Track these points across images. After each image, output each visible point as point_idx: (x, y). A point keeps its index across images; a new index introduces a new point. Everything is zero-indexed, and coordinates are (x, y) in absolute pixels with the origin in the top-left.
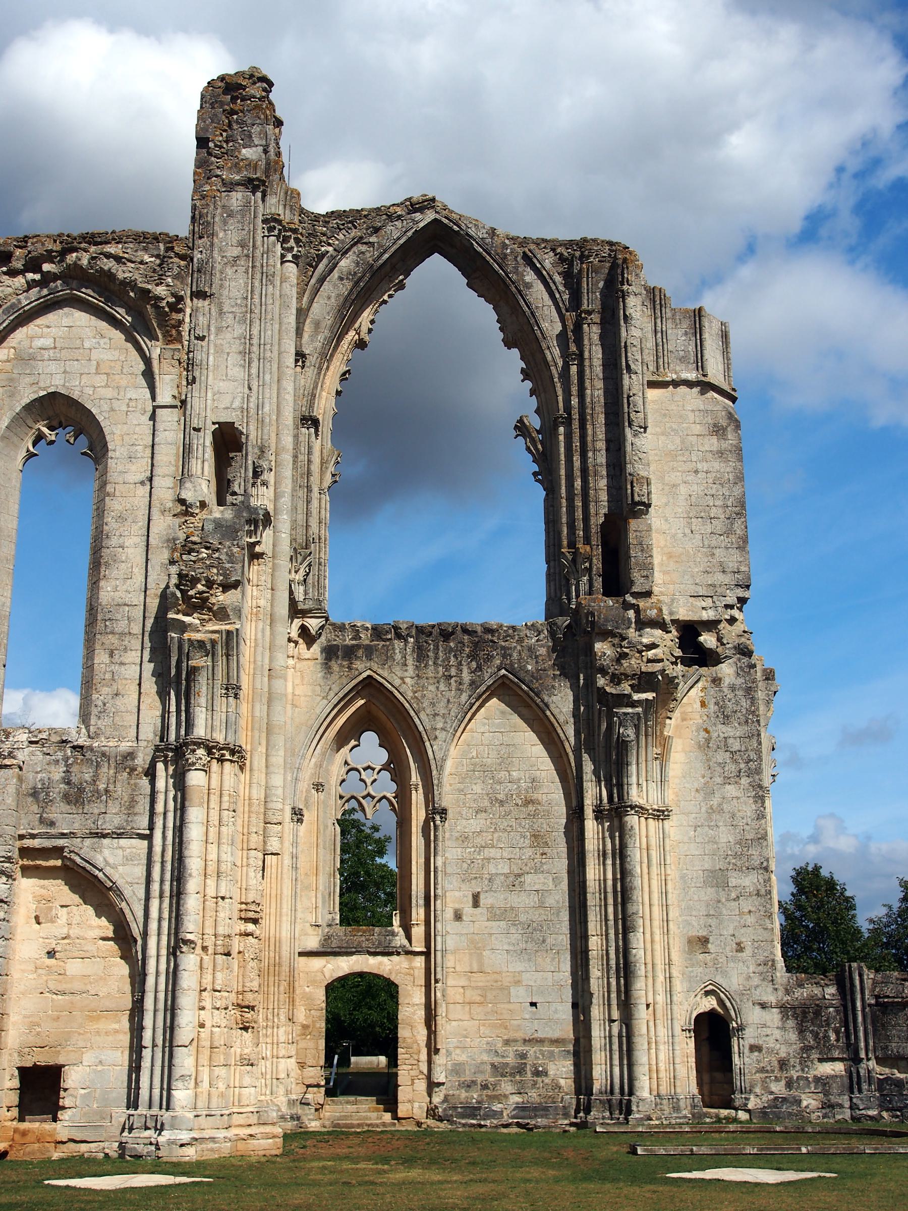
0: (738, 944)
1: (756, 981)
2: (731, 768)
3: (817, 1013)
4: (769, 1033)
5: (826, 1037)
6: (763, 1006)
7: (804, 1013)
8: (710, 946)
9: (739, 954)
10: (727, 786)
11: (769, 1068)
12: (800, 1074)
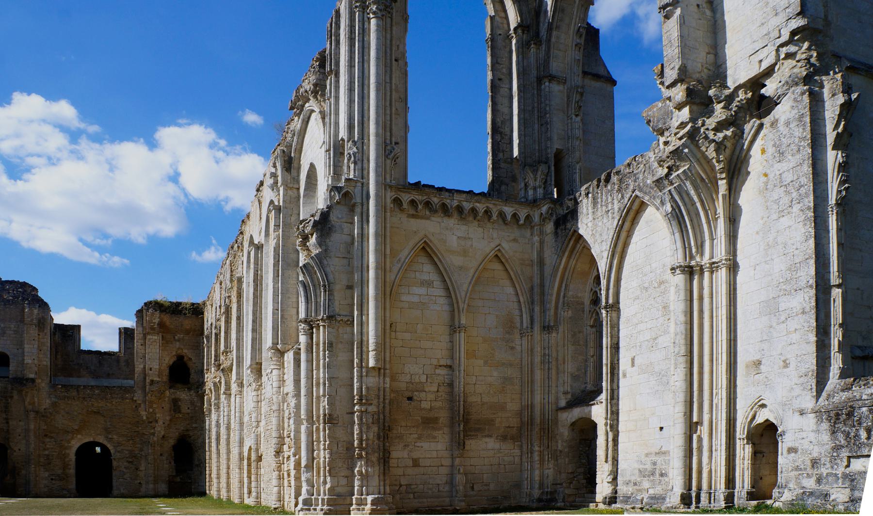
0: (784, 361)
1: (797, 391)
2: (786, 200)
3: (850, 414)
4: (805, 436)
5: (857, 436)
6: (802, 413)
7: (837, 415)
8: (762, 367)
9: (785, 370)
10: (782, 219)
11: (802, 467)
12: (830, 471)
